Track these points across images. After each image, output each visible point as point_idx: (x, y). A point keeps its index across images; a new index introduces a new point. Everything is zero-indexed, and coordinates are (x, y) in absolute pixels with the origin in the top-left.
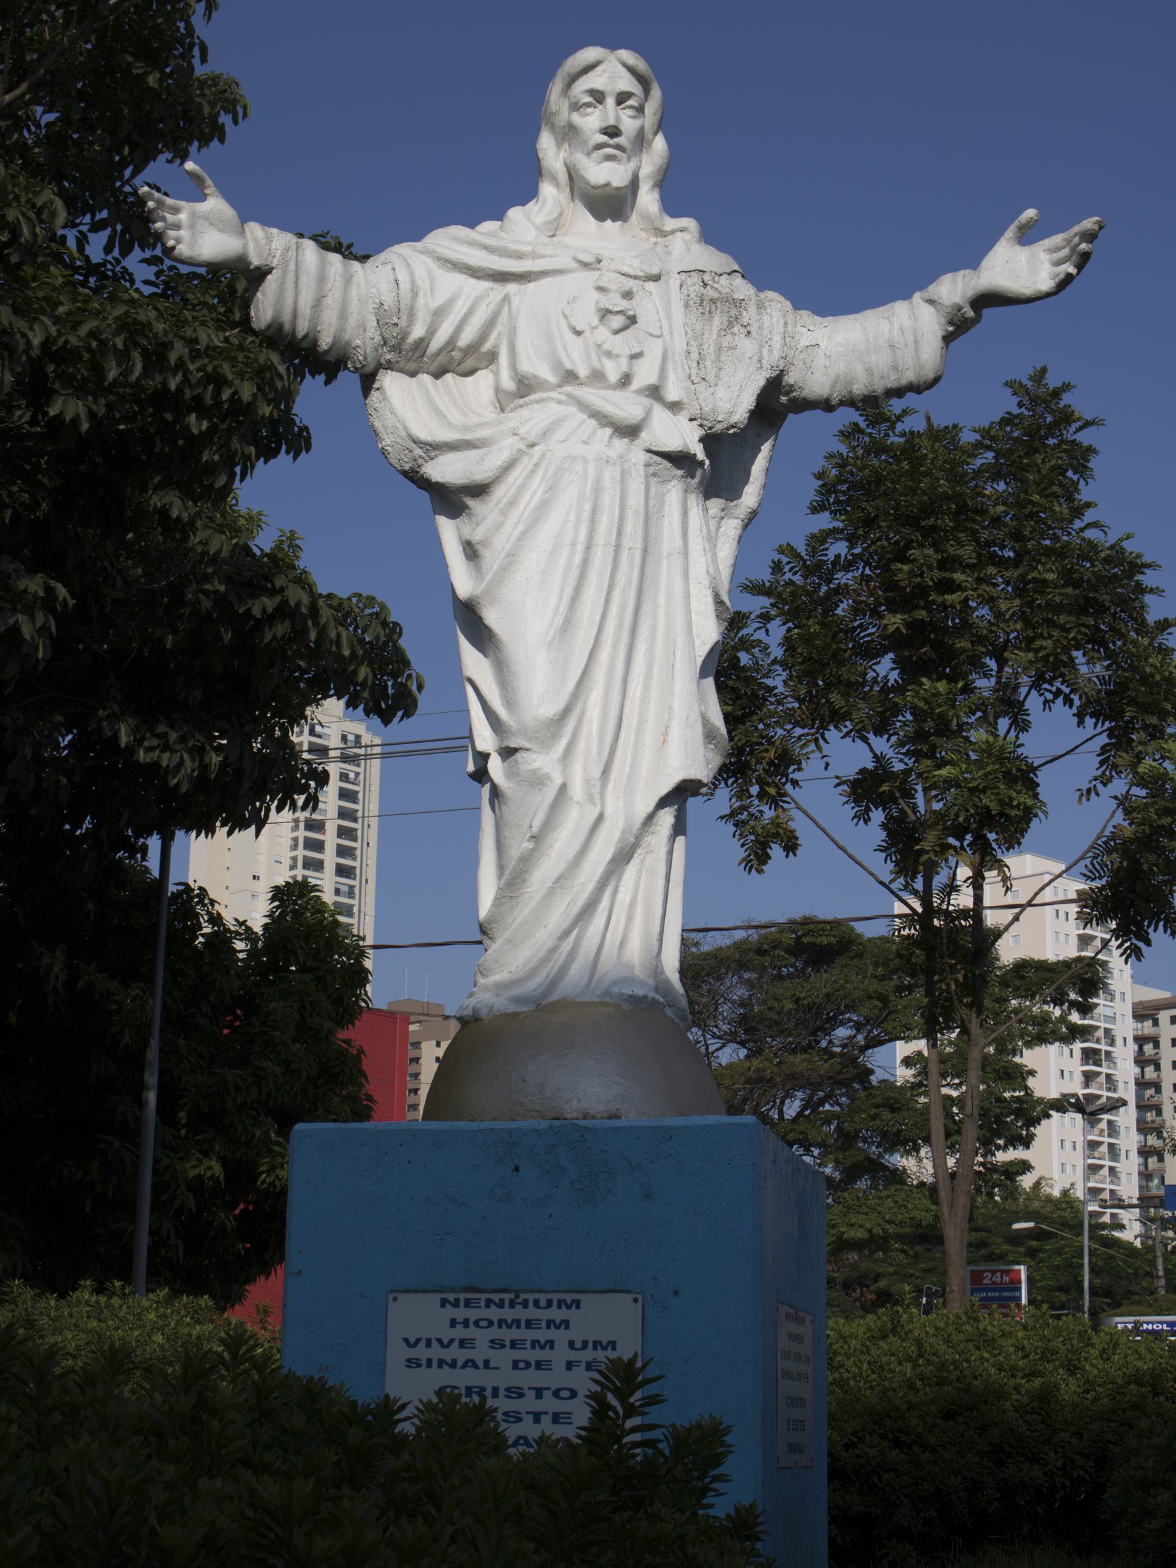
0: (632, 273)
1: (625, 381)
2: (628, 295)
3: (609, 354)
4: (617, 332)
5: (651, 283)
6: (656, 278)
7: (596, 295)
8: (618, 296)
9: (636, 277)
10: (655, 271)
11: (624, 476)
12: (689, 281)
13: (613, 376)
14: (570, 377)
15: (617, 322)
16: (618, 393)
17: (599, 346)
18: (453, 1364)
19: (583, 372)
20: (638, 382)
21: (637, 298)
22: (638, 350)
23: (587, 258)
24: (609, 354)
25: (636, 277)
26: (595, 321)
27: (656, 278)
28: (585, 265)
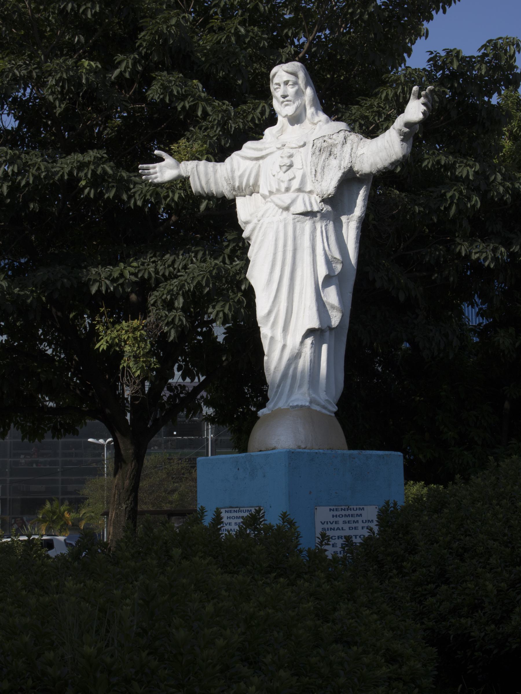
0: (294, 146)
1: (287, 190)
2: (291, 156)
3: (282, 181)
4: (285, 172)
5: (302, 148)
6: (304, 145)
7: (280, 159)
8: (286, 158)
9: (296, 148)
10: (302, 143)
11: (285, 227)
12: (318, 142)
13: (283, 190)
14: (271, 193)
15: (284, 168)
16: (287, 194)
17: (279, 179)
18: (334, 529)
19: (274, 190)
20: (293, 189)
21: (295, 157)
22: (292, 177)
23: (279, 146)
24: (282, 181)
25: (296, 148)
26: (279, 170)
27: (304, 145)
28: (279, 148)
